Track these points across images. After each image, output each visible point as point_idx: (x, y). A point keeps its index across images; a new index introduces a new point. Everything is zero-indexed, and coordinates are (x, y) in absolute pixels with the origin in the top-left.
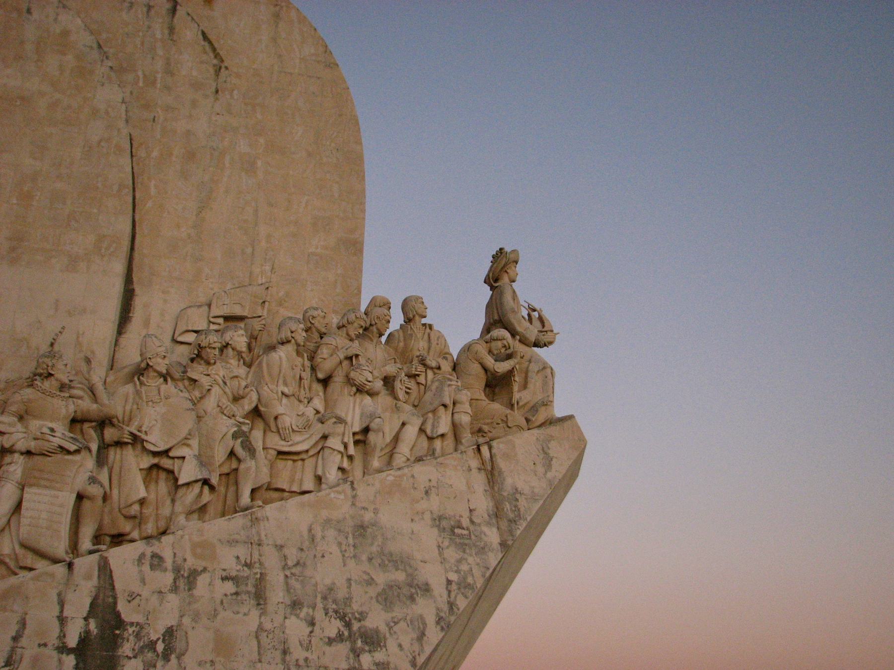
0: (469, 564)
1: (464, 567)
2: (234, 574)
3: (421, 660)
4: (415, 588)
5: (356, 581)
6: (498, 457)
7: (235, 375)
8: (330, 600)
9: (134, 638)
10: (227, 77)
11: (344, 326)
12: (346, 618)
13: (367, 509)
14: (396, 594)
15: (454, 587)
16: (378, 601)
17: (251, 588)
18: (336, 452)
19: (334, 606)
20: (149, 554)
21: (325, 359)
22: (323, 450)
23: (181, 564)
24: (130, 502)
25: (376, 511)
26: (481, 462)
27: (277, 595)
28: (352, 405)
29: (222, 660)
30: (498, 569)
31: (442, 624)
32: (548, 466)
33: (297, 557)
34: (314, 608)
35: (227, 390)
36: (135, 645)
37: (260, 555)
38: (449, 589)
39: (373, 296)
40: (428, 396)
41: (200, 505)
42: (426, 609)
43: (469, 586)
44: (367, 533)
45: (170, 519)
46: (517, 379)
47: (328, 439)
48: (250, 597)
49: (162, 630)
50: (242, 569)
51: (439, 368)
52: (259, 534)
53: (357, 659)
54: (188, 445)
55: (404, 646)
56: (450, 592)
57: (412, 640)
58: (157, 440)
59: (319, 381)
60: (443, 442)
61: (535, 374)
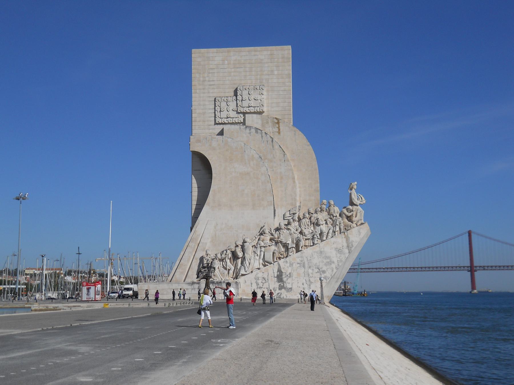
2: (299, 263)
3: (332, 275)
16: (324, 265)
17: (302, 265)
20: (285, 261)
25: (324, 249)
27: (306, 265)
30: (349, 257)
31: (337, 268)
32: (360, 235)
37: (303, 259)
42: (333, 266)
43: (342, 261)
51: (336, 216)
56: (338, 262)
58: (284, 241)
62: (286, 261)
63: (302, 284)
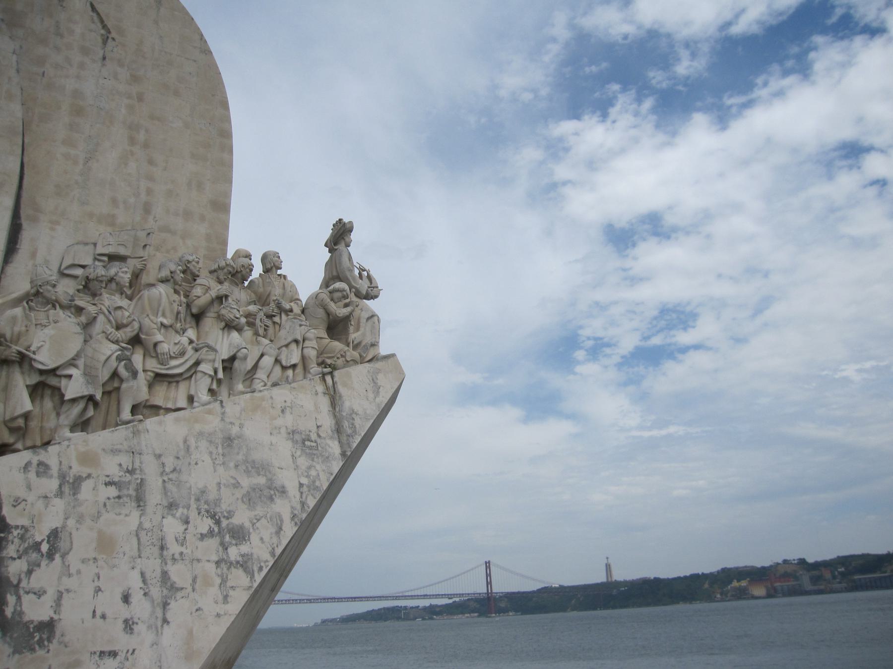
0: (317, 470)
1: (313, 473)
2: (116, 479)
3: (278, 551)
4: (274, 491)
5: (225, 485)
6: (338, 384)
7: (118, 305)
8: (202, 501)
9: (19, 540)
10: (113, 47)
11: (215, 271)
12: (216, 517)
13: (234, 424)
14: (258, 495)
15: (305, 489)
16: (243, 501)
17: (132, 492)
18: (207, 376)
19: (206, 506)
20: (35, 462)
21: (199, 297)
22: (196, 373)
23: (66, 471)
24: (16, 414)
25: (241, 426)
26: (326, 388)
27: (154, 497)
28: (221, 336)
29: (105, 557)
30: (338, 474)
31: (296, 520)
33: (173, 464)
34: (188, 509)
35: (111, 318)
36: (19, 547)
37: (141, 463)
38: (301, 491)
39: (235, 250)
40: (283, 333)
41: (85, 418)
42: (283, 507)
44: (234, 445)
45: (55, 430)
46: (352, 323)
47: (201, 364)
48: (131, 500)
49: (47, 532)
50: (124, 475)
51: (291, 311)
52: (138, 443)
53: (225, 551)
54: (75, 366)
55: (264, 540)
56: (302, 493)
57: (271, 534)
58: (45, 359)
59: (193, 315)
60: (294, 371)
61: (365, 320)
62: (40, 464)
63: (120, 596)
